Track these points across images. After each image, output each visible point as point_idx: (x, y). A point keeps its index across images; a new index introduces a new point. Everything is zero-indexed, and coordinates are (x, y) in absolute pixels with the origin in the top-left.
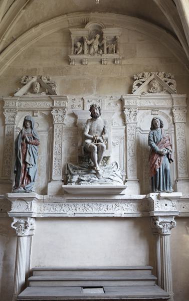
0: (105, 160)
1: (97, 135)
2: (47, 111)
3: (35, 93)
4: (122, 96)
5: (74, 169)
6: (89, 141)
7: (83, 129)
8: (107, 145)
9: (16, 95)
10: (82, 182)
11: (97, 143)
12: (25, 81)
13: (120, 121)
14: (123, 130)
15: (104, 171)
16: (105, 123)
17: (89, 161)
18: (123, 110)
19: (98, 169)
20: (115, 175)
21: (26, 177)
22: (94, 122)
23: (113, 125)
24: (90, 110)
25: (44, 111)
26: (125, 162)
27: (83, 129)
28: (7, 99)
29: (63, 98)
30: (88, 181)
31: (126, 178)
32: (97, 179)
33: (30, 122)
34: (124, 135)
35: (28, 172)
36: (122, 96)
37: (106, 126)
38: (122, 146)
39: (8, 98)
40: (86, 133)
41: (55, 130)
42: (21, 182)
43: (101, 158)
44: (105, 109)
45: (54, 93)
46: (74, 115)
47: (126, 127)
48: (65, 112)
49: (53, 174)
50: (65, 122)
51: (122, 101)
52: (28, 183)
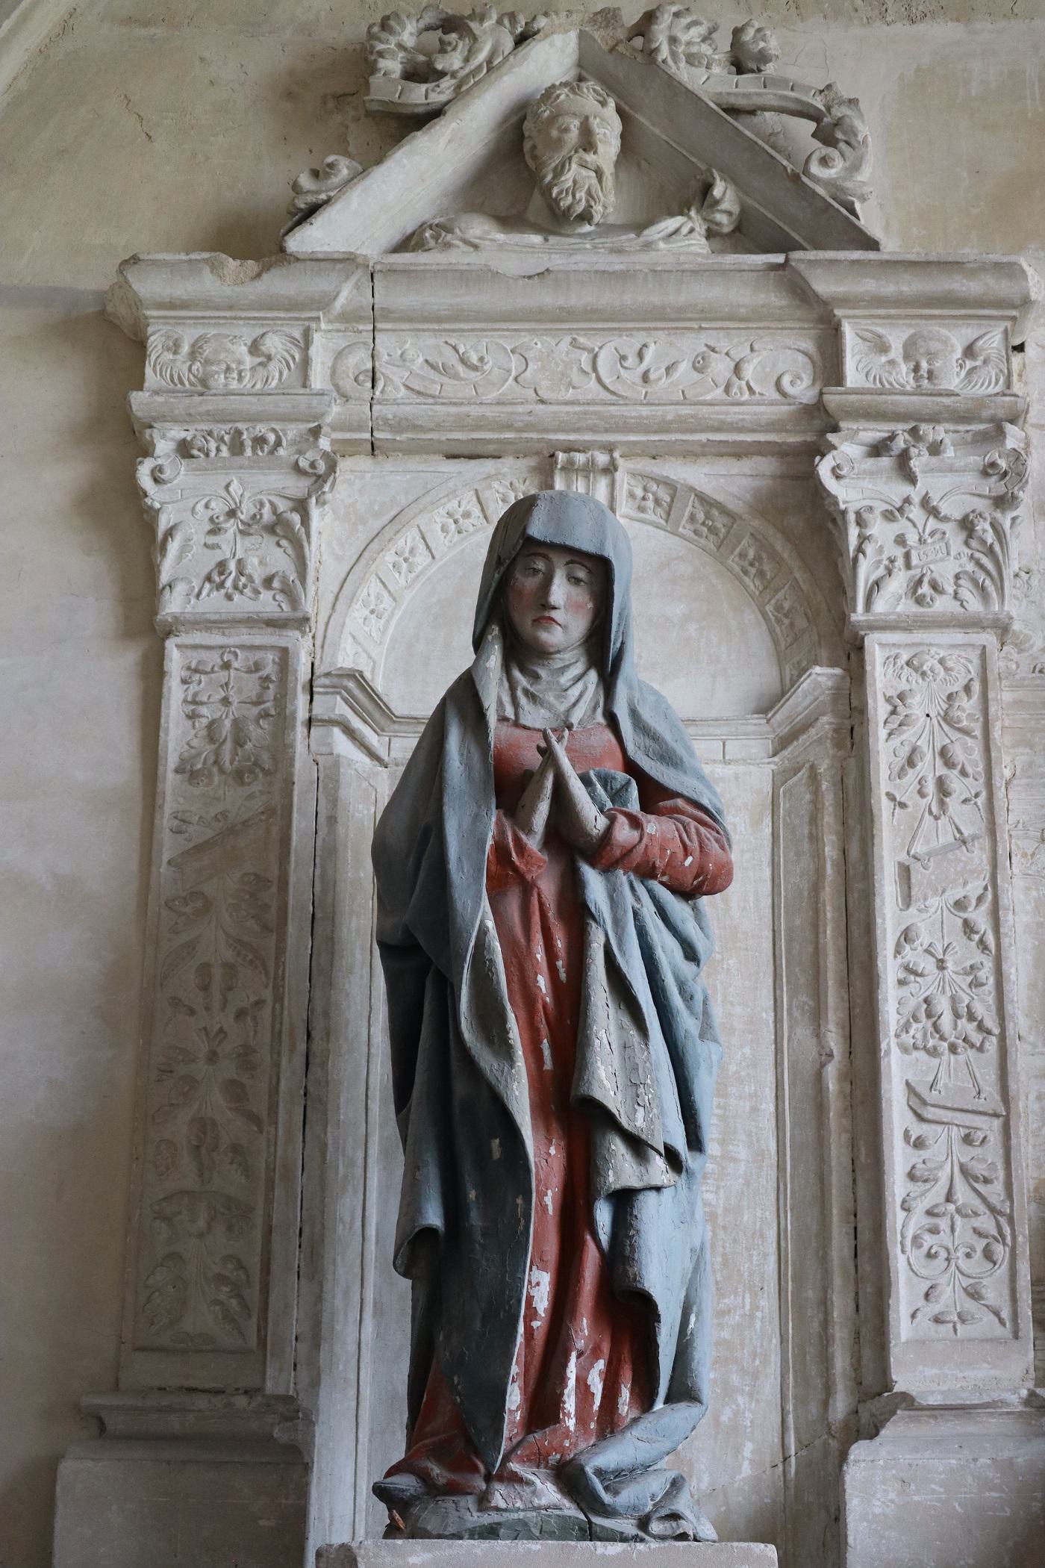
2: (739, 452)
3: (558, 219)
9: (306, 240)
12: (420, 73)
21: (584, 1329)
25: (689, 453)
28: (181, 289)
29: (972, 287)
33: (599, 574)
35: (620, 1255)
39: (207, 284)
41: (879, 710)
42: (515, 1398)
45: (838, 227)
49: (903, 1328)
50: (1014, 608)
52: (608, 1424)
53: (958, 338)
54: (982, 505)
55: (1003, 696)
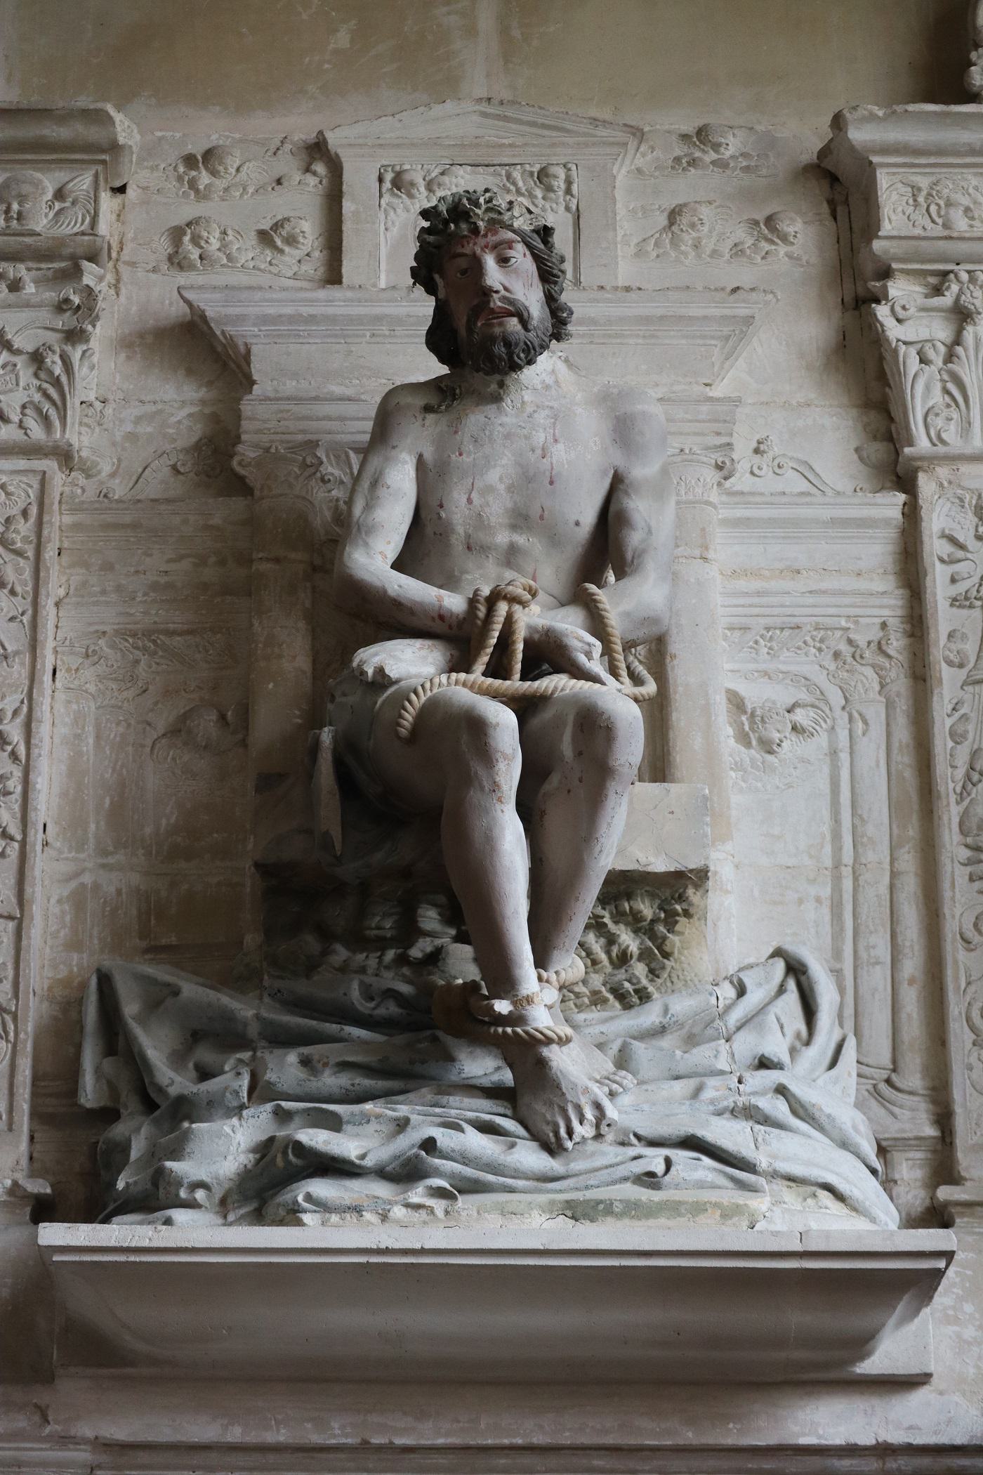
0: (635, 922)
1: (518, 583)
4: (838, 122)
5: (195, 1037)
6: (410, 663)
7: (321, 518)
8: (658, 713)
10: (321, 1188)
11: (515, 684)
13: (827, 437)
14: (877, 551)
15: (623, 1061)
16: (624, 430)
17: (409, 931)
18: (855, 287)
19: (542, 1018)
20: (780, 1108)
22: (476, 419)
23: (741, 481)
24: (428, 270)
26: (912, 965)
27: (321, 518)
29: (61, 133)
30: (405, 1173)
31: (944, 1168)
32: (528, 1156)
34: (887, 603)
36: (838, 122)
37: (642, 472)
38: (872, 751)
40: (375, 560)
43: (577, 869)
44: (621, 282)
46: (201, 348)
47: (912, 514)
48: (88, 307)
50: (79, 437)
51: (839, 185)
53: (49, 183)
54: (52, 338)
55: (57, 519)
